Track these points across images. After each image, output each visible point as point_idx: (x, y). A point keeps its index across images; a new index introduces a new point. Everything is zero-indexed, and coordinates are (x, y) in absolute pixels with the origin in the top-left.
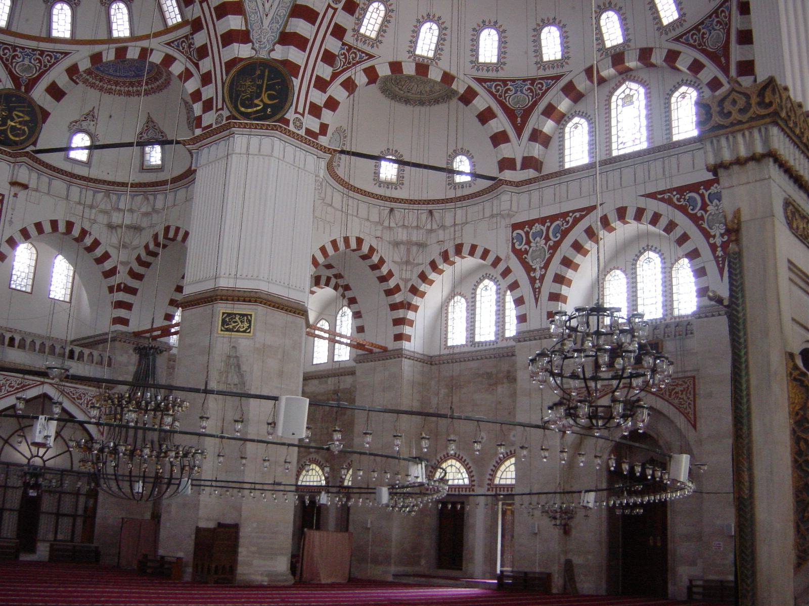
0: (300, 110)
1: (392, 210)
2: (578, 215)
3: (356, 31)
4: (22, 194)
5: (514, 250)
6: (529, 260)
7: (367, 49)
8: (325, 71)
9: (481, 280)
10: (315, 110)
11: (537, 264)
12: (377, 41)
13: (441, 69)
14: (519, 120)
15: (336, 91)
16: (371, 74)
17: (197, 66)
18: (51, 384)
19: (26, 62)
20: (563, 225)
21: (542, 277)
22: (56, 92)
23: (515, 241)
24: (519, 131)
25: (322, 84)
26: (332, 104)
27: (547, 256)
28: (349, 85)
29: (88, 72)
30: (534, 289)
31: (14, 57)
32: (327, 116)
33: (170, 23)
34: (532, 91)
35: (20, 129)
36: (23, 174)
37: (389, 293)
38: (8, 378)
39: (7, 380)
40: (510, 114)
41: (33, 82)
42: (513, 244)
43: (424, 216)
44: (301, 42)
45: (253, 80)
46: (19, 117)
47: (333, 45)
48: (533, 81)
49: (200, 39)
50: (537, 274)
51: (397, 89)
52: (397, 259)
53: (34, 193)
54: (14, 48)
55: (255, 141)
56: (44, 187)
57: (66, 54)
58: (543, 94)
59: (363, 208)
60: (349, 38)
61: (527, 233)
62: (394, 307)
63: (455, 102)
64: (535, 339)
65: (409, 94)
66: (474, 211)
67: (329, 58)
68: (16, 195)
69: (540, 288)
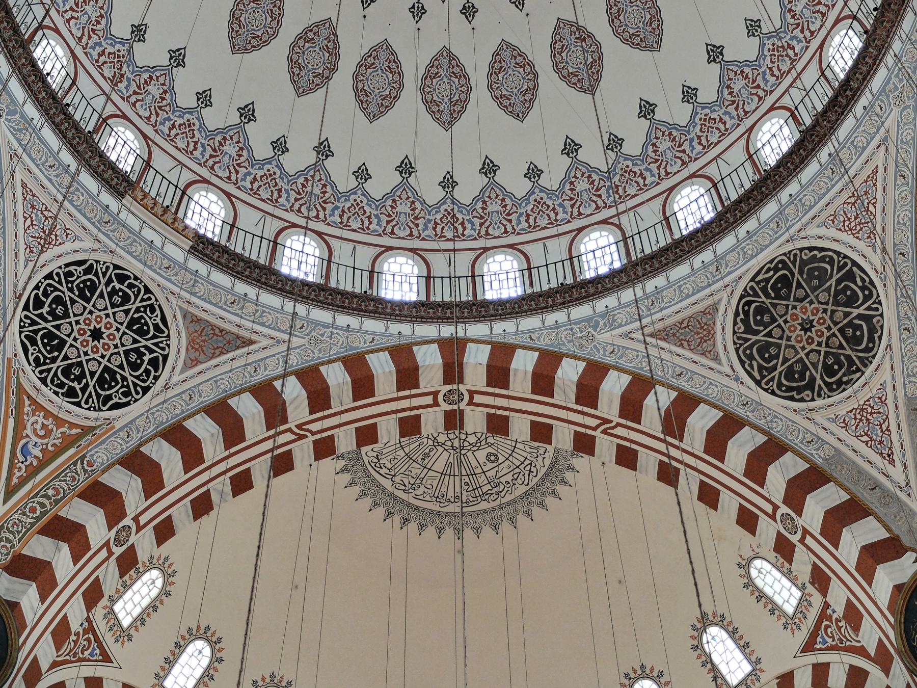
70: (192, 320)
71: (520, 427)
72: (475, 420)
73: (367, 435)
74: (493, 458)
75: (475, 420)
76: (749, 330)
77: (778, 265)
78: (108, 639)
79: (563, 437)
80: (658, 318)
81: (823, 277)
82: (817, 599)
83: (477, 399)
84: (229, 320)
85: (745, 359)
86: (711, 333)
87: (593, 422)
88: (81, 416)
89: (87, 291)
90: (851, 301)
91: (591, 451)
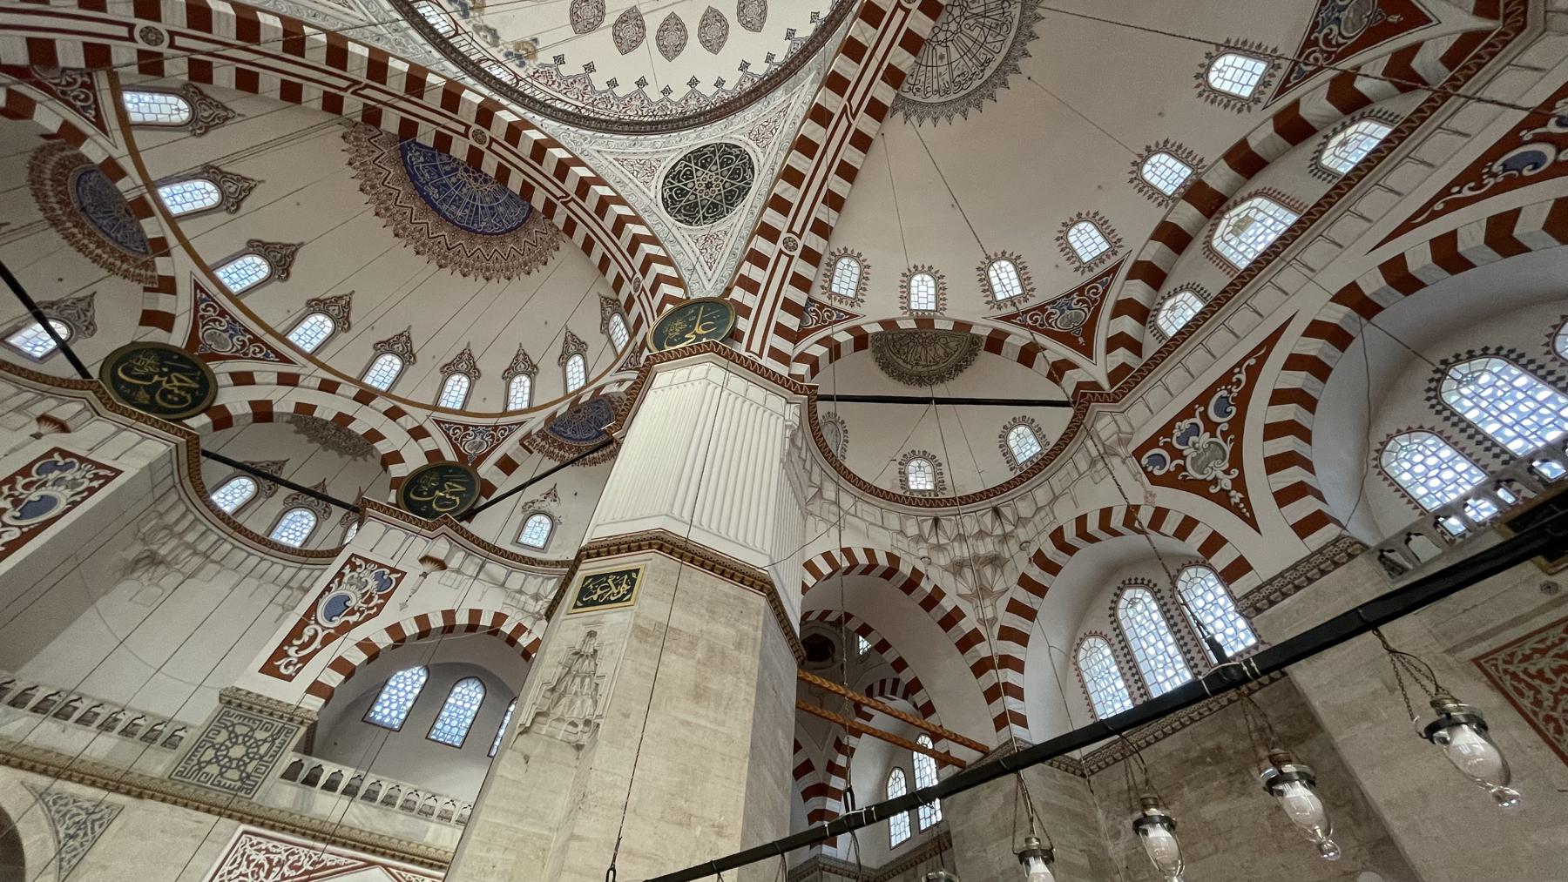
1: (936, 521)
2: (1252, 361)
3: (827, 290)
4: (436, 575)
5: (1154, 480)
6: (1193, 473)
7: (848, 308)
9: (1118, 596)
11: (1217, 470)
13: (951, 320)
14: (1081, 340)
18: (385, 867)
19: (478, 439)
20: (1230, 392)
21: (1240, 484)
22: (507, 465)
23: (1150, 469)
24: (1088, 351)
27: (1228, 448)
29: (542, 434)
30: (1235, 510)
31: (464, 436)
34: (1084, 302)
35: (450, 500)
36: (440, 549)
37: (966, 643)
38: (295, 849)
39: (293, 854)
40: (1065, 338)
41: (481, 459)
42: (1150, 475)
43: (988, 519)
45: (687, 319)
46: (450, 487)
48: (1081, 290)
50: (1226, 483)
51: (901, 362)
52: (965, 591)
53: (454, 575)
54: (466, 427)
56: (471, 569)
57: (521, 424)
58: (1103, 297)
59: (893, 521)
61: (1168, 447)
62: (980, 668)
63: (985, 357)
64: (1298, 588)
65: (920, 368)
66: (1060, 477)
68: (425, 575)
69: (1246, 500)
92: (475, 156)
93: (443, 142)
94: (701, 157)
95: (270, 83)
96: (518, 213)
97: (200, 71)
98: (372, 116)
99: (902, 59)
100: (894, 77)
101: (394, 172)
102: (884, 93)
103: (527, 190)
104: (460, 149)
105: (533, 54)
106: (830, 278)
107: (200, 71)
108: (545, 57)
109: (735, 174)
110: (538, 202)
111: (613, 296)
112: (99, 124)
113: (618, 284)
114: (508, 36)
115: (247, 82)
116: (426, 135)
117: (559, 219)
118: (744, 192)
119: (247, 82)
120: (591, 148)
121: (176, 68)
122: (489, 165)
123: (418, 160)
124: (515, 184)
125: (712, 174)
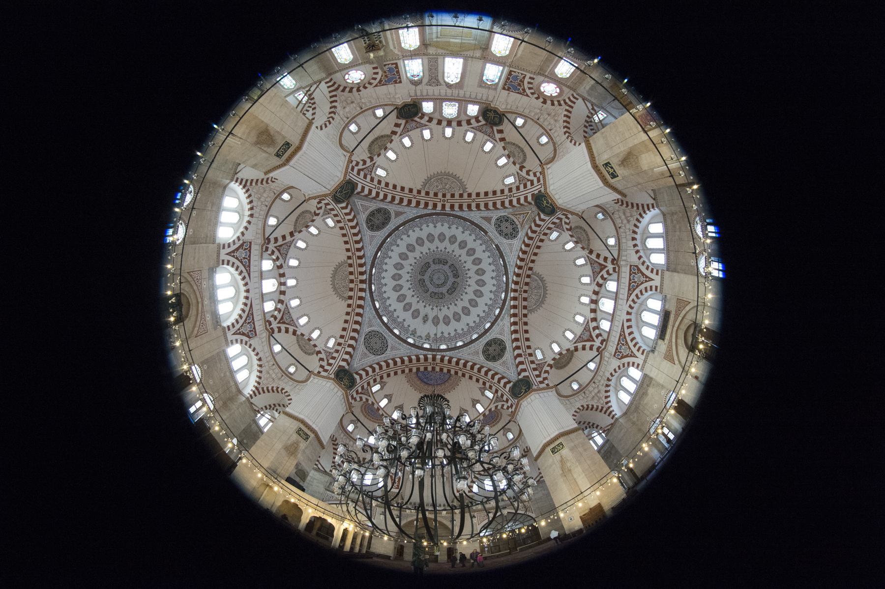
0: (536, 384)
3: (537, 360)
8: (537, 373)
10: (541, 382)
12: (544, 358)
15: (544, 375)
16: (550, 366)
17: (504, 401)
25: (538, 376)
26: (545, 379)
28: (547, 372)
32: (546, 382)
33: (491, 398)
44: (524, 370)
47: (533, 366)
49: (499, 394)
55: (529, 399)
60: (537, 362)
67: (535, 369)
70: (490, 223)
71: (432, 194)
72: (440, 195)
73: (461, 195)
74: (437, 187)
75: (440, 195)
76: (388, 216)
77: (385, 226)
78: (516, 175)
79: (423, 193)
80: (405, 215)
81: (376, 228)
82: (373, 175)
83: (439, 200)
84: (484, 221)
85: (389, 212)
86: (396, 214)
87: (417, 197)
88: (513, 217)
89: (506, 235)
90: (371, 225)
91: (418, 190)
92: (433, 369)
93: (426, 369)
94: (488, 344)
95: (392, 374)
96: (447, 376)
97: (382, 378)
98: (411, 370)
99: (525, 303)
100: (525, 307)
101: (416, 379)
102: (525, 312)
103: (449, 371)
104: (430, 369)
105: (430, 337)
106: (536, 356)
107: (382, 378)
108: (432, 336)
109: (500, 345)
110: (453, 372)
111: (483, 386)
112: (370, 396)
113: (484, 383)
114: (423, 336)
115: (389, 375)
116: (422, 369)
117: (460, 373)
118: (505, 348)
119: (389, 375)
120: (460, 354)
121: (378, 379)
122: (438, 369)
123: (420, 374)
124: (445, 370)
125: (494, 347)
